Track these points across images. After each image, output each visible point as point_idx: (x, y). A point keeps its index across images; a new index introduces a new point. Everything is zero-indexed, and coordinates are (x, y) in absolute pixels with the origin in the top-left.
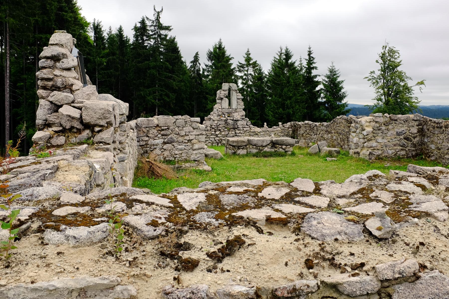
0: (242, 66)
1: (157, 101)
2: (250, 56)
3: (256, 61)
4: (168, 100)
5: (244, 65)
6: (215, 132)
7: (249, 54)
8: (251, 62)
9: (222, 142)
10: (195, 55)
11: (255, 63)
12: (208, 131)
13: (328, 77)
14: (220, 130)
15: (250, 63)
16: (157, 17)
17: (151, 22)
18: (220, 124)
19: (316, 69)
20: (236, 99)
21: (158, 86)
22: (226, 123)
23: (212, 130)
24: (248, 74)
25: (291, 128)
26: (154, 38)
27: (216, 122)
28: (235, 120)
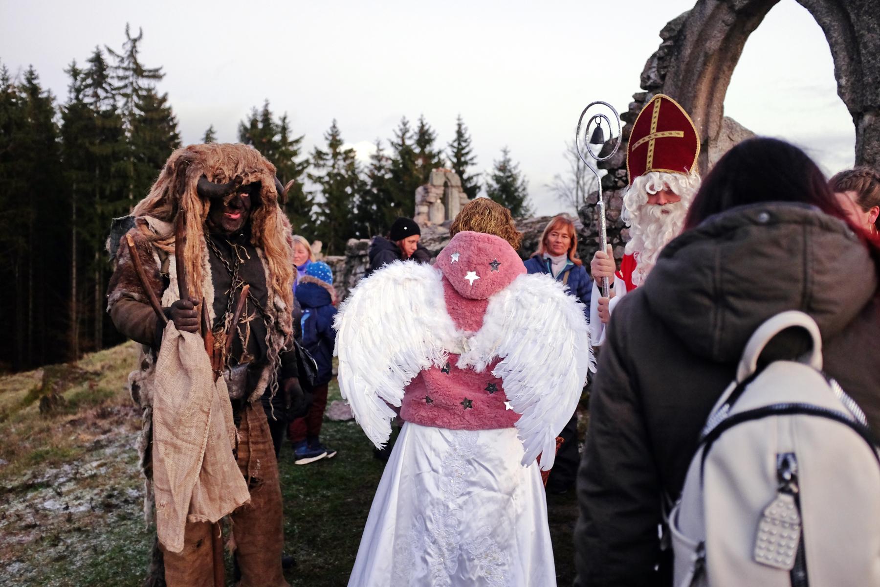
2: (338, 138)
5: (327, 154)
8: (342, 149)
13: (498, 179)
16: (132, 52)
17: (119, 59)
19: (473, 164)
26: (125, 95)
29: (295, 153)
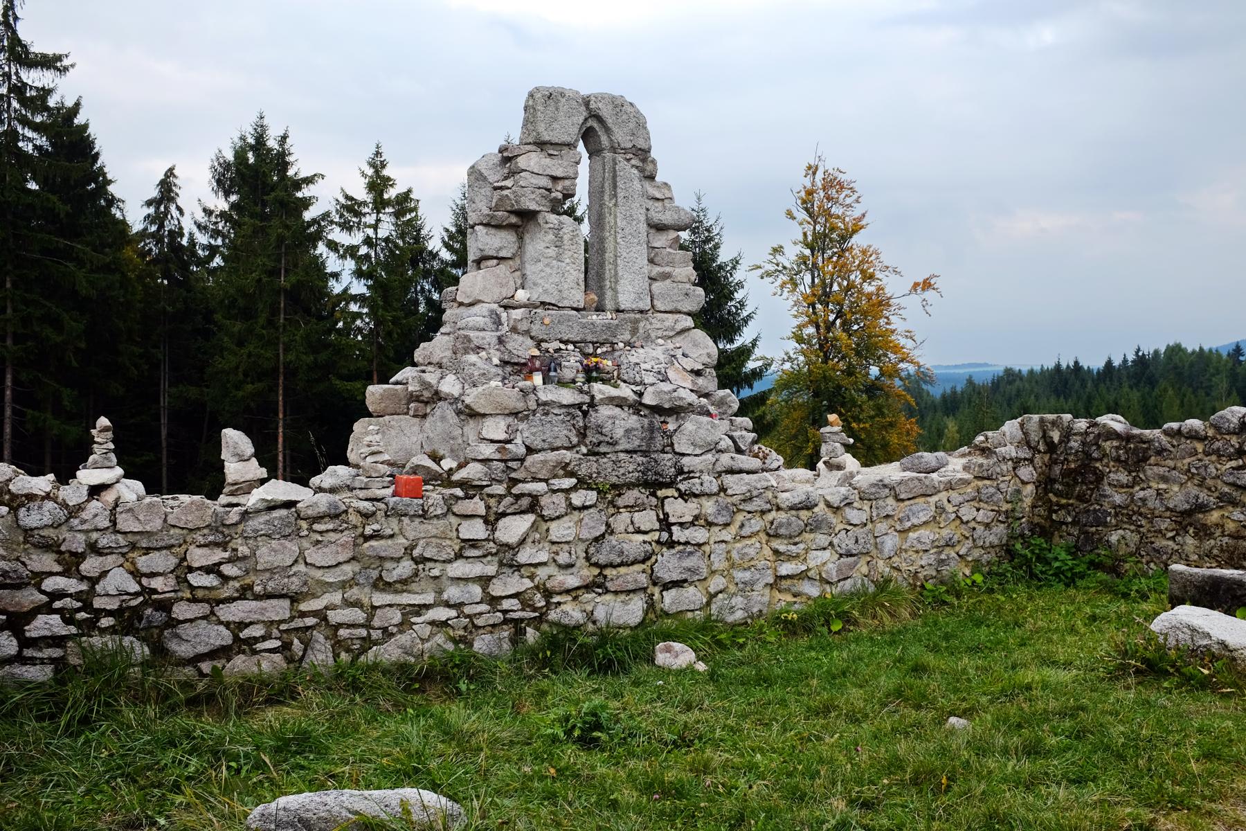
0: (351, 207)
1: (9, 342)
2: (385, 172)
3: (410, 191)
4: (59, 339)
5: (365, 203)
6: (491, 521)
7: (383, 165)
8: (391, 194)
9: (553, 615)
10: (162, 177)
11: (405, 197)
12: (424, 515)
14: (534, 505)
15: (386, 196)
18: (530, 450)
20: (643, 227)
21: (14, 284)
22: (582, 435)
23: (460, 508)
24: (376, 238)
25: (1031, 461)
27: (496, 429)
28: (657, 410)
29: (306, 203)
